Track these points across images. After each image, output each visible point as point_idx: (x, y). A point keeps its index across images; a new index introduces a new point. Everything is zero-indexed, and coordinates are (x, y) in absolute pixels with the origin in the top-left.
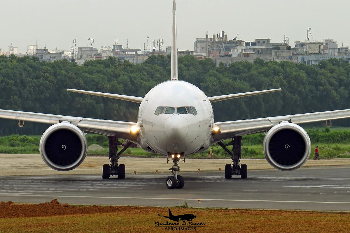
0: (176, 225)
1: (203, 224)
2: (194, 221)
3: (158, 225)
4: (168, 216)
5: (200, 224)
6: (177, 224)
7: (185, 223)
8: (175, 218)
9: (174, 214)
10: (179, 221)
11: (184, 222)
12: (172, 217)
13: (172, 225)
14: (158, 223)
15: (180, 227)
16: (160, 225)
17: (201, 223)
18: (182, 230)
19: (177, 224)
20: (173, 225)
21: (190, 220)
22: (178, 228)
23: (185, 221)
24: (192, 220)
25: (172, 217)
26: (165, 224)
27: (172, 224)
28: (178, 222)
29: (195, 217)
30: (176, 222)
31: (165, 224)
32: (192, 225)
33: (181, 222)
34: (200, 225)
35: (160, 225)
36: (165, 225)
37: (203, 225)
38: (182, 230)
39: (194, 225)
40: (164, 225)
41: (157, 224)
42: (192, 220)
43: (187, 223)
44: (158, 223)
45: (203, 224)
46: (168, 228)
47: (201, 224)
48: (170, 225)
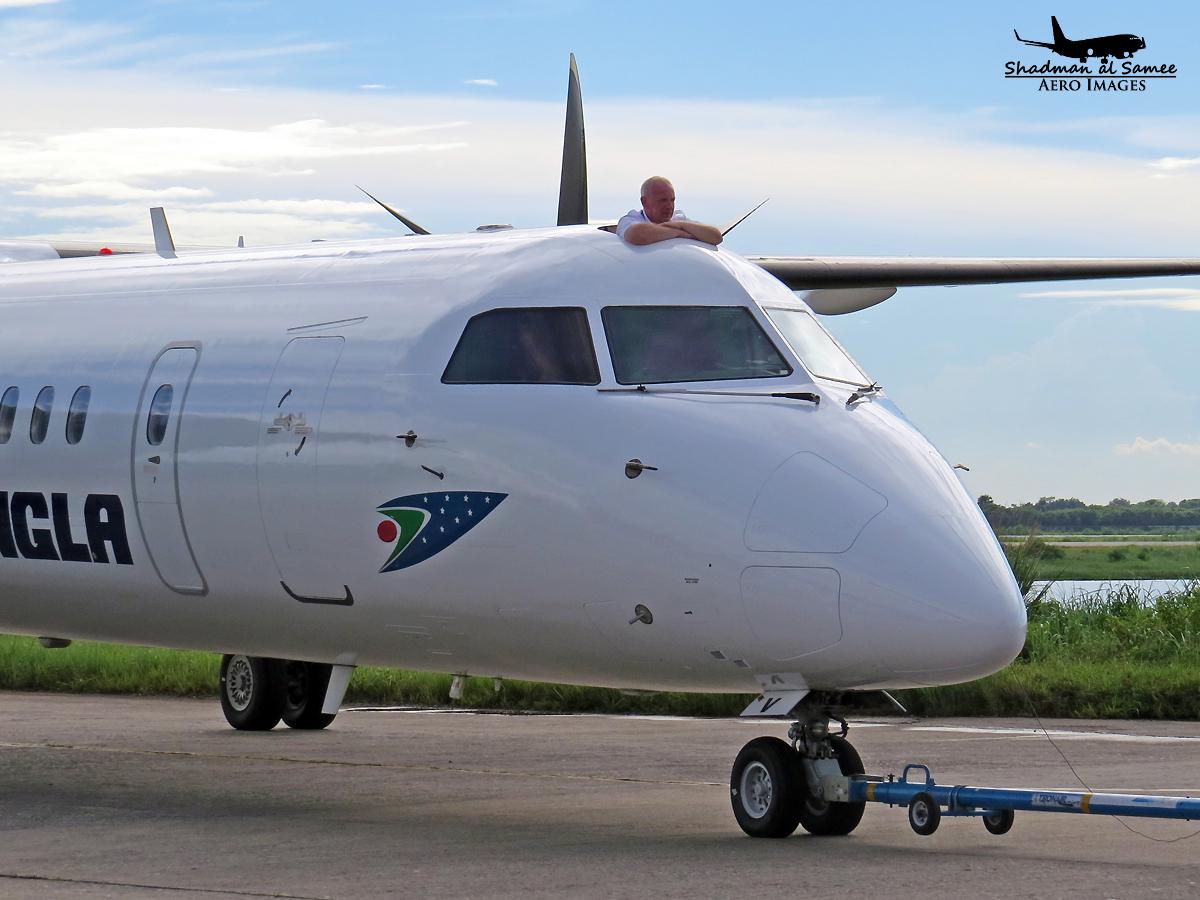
0: (1079, 74)
1: (1170, 71)
2: (1140, 58)
3: (1015, 74)
6: (1082, 70)
7: (1108, 66)
9: (1072, 34)
10: (1089, 59)
11: (1105, 61)
12: (1062, 45)
13: (1064, 73)
14: (1015, 67)
15: (1093, 81)
16: (1022, 73)
18: (1100, 88)
19: (1082, 70)
20: (1069, 74)
21: (1126, 54)
23: (1110, 58)
24: (1131, 56)
25: (1062, 45)
26: (1041, 71)
27: (1065, 68)
28: (1083, 60)
29: (1144, 47)
30: (1076, 61)
31: (1041, 71)
32: (1131, 74)
33: (1094, 63)
34: (1160, 74)
35: (1022, 73)
36: (1039, 74)
37: (1168, 74)
38: (1100, 88)
39: (1138, 74)
40: (1035, 74)
41: (1014, 70)
42: (1131, 56)
43: (1117, 64)
44: (1015, 67)
45: (1170, 71)
47: (1162, 71)
48: (1058, 74)
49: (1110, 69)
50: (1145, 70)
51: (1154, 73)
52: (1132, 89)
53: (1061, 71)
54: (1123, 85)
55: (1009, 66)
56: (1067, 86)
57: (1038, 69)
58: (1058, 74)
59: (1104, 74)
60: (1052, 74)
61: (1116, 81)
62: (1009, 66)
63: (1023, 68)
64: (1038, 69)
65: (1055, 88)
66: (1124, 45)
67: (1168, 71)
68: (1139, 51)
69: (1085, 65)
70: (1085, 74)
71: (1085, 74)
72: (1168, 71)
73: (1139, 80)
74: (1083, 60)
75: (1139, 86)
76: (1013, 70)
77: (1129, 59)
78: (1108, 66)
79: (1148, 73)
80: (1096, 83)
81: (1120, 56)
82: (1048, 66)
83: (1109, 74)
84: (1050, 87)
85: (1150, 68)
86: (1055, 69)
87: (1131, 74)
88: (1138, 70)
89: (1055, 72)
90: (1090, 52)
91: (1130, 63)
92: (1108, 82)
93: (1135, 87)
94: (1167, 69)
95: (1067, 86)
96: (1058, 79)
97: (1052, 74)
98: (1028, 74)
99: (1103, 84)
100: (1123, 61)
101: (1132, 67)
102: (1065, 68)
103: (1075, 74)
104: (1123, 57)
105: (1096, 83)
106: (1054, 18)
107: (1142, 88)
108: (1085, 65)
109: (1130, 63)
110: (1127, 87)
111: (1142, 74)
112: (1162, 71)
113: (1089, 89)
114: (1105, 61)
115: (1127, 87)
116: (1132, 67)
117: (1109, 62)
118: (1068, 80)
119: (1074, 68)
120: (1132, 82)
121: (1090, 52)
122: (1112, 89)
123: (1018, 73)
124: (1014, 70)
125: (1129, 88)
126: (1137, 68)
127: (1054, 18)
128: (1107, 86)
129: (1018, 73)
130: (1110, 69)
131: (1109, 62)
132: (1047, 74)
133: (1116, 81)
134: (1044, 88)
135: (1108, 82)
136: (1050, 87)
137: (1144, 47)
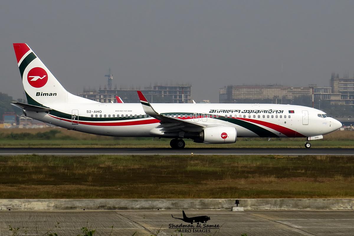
2: (209, 223)
3: (172, 227)
4: (182, 218)
6: (192, 226)
7: (199, 225)
10: (193, 223)
11: (198, 224)
12: (186, 219)
13: (186, 227)
14: (172, 225)
19: (192, 226)
20: (187, 228)
21: (204, 222)
23: (200, 223)
29: (210, 219)
30: (190, 224)
31: (179, 226)
33: (195, 224)
34: (214, 227)
35: (174, 227)
36: (179, 227)
37: (217, 228)
40: (178, 227)
42: (206, 222)
43: (202, 224)
45: (217, 227)
47: (215, 226)
55: (170, 225)
56: (187, 231)
60: (183, 227)
69: (192, 224)
70: (192, 227)
71: (192, 227)
76: (171, 226)
78: (199, 225)
81: (203, 222)
84: (182, 231)
86: (183, 226)
90: (194, 221)
94: (217, 226)
95: (187, 231)
99: (198, 230)
102: (186, 226)
105: (196, 230)
108: (192, 225)
112: (215, 226)
113: (194, 232)
116: (206, 225)
121: (194, 221)
128: (199, 231)
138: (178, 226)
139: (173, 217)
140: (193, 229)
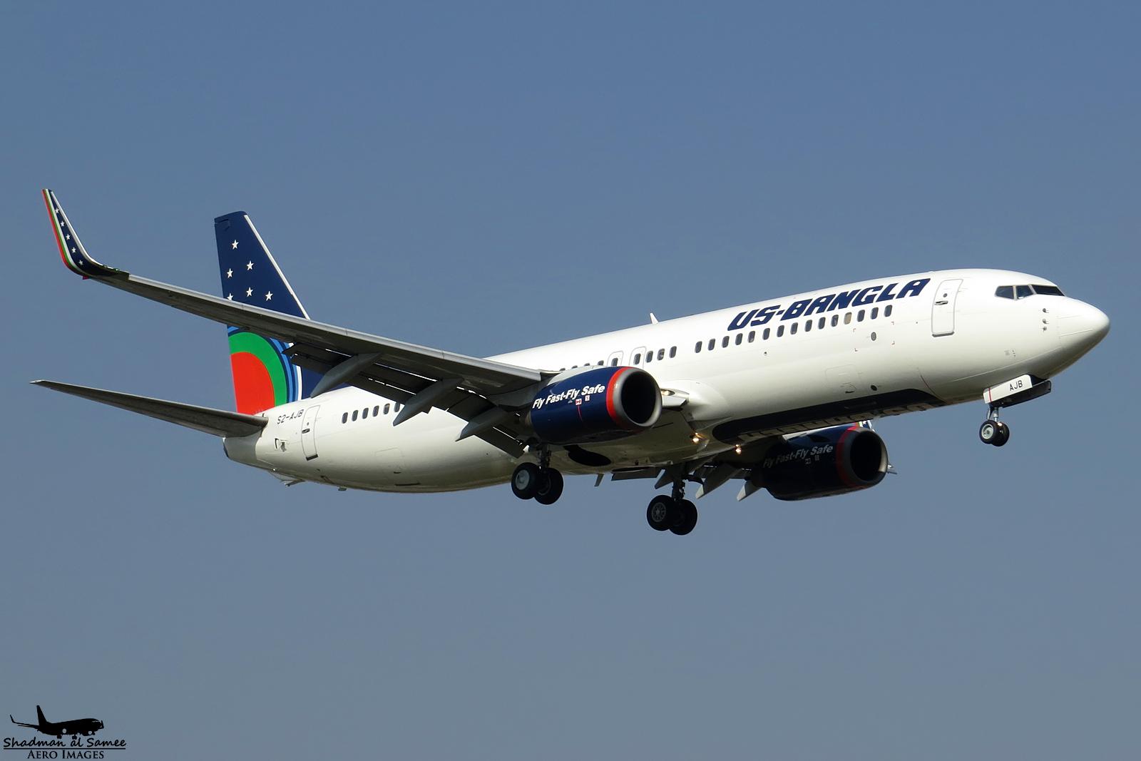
0: (56, 747)
1: (121, 744)
2: (99, 735)
3: (10, 747)
4: (38, 724)
5: (113, 743)
6: (59, 744)
7: (77, 741)
8: (54, 729)
9: (51, 719)
11: (75, 738)
12: (44, 726)
13: (45, 746)
14: (11, 742)
15: (66, 751)
16: (15, 746)
17: (117, 741)
18: (71, 757)
19: (59, 744)
20: (49, 747)
21: (90, 732)
22: (60, 752)
23: (78, 735)
24: (93, 734)
25: (44, 726)
26: (29, 744)
27: (46, 742)
28: (59, 737)
29: (103, 727)
30: (55, 738)
31: (29, 744)
32: (94, 747)
33: (67, 739)
34: (114, 747)
35: (15, 746)
36: (28, 747)
37: (120, 747)
38: (71, 757)
39: (98, 747)
40: (25, 747)
41: (10, 744)
42: (93, 734)
43: (83, 739)
44: (11, 742)
45: (121, 744)
46: (35, 752)
47: (115, 744)
48: (41, 746)
49: (79, 743)
50: (104, 743)
51: (110, 746)
52: (94, 758)
53: (43, 745)
54: (88, 756)
55: (7, 741)
56: (48, 755)
57: (27, 743)
58: (41, 746)
59: (74, 747)
60: (37, 747)
61: (83, 752)
62: (7, 741)
63: (17, 742)
64: (27, 743)
65: (39, 756)
66: (88, 726)
67: (120, 744)
68: (99, 730)
69: (59, 740)
70: (61, 746)
71: (61, 746)
72: (120, 744)
73: (99, 751)
74: (59, 737)
75: (98, 754)
77: (92, 736)
78: (77, 741)
79: (106, 746)
80: (69, 753)
81: (86, 734)
82: (34, 741)
83: (77, 747)
84: (35, 757)
85: (107, 742)
86: (39, 743)
87: (94, 747)
88: (99, 744)
89: (43, 745)
90: (64, 731)
91: (93, 739)
92: (77, 752)
93: (96, 756)
94: (119, 743)
95: (48, 755)
96: (41, 750)
97: (37, 747)
98: (20, 747)
99: (74, 754)
100: (88, 737)
101: (94, 742)
102: (46, 742)
103: (54, 747)
104: (88, 735)
105: (69, 753)
106: (38, 708)
107: (101, 757)
109: (93, 739)
110: (90, 756)
111: (101, 746)
112: (115, 744)
114: (75, 738)
115: (90, 756)
116: (94, 742)
117: (78, 739)
118: (49, 751)
119: (53, 743)
120: (94, 752)
121: (64, 731)
122: (80, 757)
123: (13, 745)
124: (10, 744)
125: (92, 756)
126: (98, 743)
127: (38, 708)
128: (76, 756)
129: (13, 745)
130: (79, 743)
131: (78, 739)
132: (33, 746)
133: (83, 752)
134: (31, 757)
135: (77, 752)
136: (35, 757)
137: (103, 727)
138: (25, 744)
139: (12, 720)
140: (62, 751)
